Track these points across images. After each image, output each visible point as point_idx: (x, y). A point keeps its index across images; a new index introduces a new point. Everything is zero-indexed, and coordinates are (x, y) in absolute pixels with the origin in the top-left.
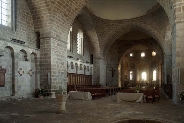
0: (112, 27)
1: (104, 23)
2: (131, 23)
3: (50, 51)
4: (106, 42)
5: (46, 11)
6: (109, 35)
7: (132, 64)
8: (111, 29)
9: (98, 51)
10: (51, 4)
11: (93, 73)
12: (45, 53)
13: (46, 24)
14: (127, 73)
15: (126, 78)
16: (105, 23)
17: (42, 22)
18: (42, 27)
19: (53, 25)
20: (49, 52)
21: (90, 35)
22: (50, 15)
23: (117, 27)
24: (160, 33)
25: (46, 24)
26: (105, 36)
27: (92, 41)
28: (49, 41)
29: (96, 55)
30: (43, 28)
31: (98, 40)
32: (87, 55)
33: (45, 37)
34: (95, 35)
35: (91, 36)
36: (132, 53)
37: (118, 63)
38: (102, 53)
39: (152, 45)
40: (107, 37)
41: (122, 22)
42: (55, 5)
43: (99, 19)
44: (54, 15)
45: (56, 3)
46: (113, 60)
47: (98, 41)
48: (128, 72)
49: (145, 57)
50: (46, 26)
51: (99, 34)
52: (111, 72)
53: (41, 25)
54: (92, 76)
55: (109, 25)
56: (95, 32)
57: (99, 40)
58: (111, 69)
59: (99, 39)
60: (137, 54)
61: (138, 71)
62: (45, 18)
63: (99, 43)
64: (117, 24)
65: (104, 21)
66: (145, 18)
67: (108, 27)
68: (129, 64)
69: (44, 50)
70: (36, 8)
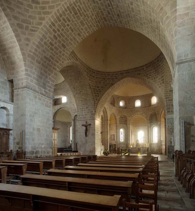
4: (37, 46)
6: (42, 29)
7: (122, 118)
8: (45, 13)
9: (22, 71)
14: (115, 130)
15: (114, 140)
23: (59, 4)
26: (34, 31)
29: (19, 80)
36: (122, 101)
39: (150, 78)
40: (37, 33)
46: (87, 108)
48: (116, 129)
49: (141, 107)
51: (16, 22)
52: (84, 127)
58: (85, 123)
59: (17, 36)
60: (130, 101)
61: (131, 127)
67: (38, 5)
68: (118, 118)
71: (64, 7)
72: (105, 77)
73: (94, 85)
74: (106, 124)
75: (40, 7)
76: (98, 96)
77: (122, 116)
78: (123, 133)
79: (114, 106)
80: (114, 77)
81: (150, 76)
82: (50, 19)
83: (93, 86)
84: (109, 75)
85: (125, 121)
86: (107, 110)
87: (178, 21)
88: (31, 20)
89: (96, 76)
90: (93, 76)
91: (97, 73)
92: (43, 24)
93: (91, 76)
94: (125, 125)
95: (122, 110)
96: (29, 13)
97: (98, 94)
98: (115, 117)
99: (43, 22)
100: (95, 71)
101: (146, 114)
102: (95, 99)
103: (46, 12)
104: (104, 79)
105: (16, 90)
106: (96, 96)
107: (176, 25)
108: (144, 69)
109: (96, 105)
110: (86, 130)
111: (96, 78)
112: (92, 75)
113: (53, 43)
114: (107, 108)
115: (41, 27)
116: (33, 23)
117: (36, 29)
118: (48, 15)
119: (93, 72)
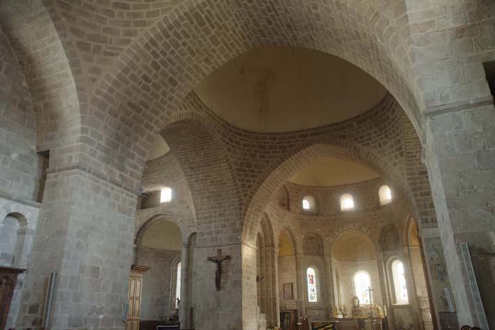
0: (144, 11)
4: (115, 83)
7: (310, 238)
14: (294, 272)
15: (293, 298)
26: (112, 54)
31: (69, 70)
37: (238, 223)
39: (368, 144)
46: (220, 215)
47: (71, 78)
48: (297, 268)
52: (213, 263)
54: (21, 271)
56: (51, 25)
58: (214, 254)
60: (326, 198)
61: (335, 264)
67: (126, 11)
68: (300, 238)
71: (179, 14)
72: (265, 143)
73: (239, 162)
74: (270, 254)
75: (128, 14)
76: (250, 187)
77: (310, 235)
78: (314, 279)
79: (289, 209)
80: (286, 143)
81: (370, 142)
82: (147, 33)
83: (236, 163)
84: (275, 139)
85: (319, 247)
86: (271, 219)
87: (415, 35)
88: (108, 36)
89: (243, 142)
90: (236, 142)
91: (245, 136)
92: (131, 43)
93: (232, 141)
94: (318, 258)
95: (310, 220)
96: (105, 24)
97: (249, 181)
98: (292, 235)
99: (133, 39)
100: (243, 130)
101: (370, 229)
102: (242, 194)
103: (141, 21)
104: (263, 147)
106: (243, 186)
107: (410, 42)
108: (352, 126)
109: (243, 207)
110: (219, 272)
111: (244, 145)
112: (234, 140)
113: (150, 76)
114: (271, 215)
115: (129, 46)
117: (118, 51)
118: (145, 28)
119: (236, 133)
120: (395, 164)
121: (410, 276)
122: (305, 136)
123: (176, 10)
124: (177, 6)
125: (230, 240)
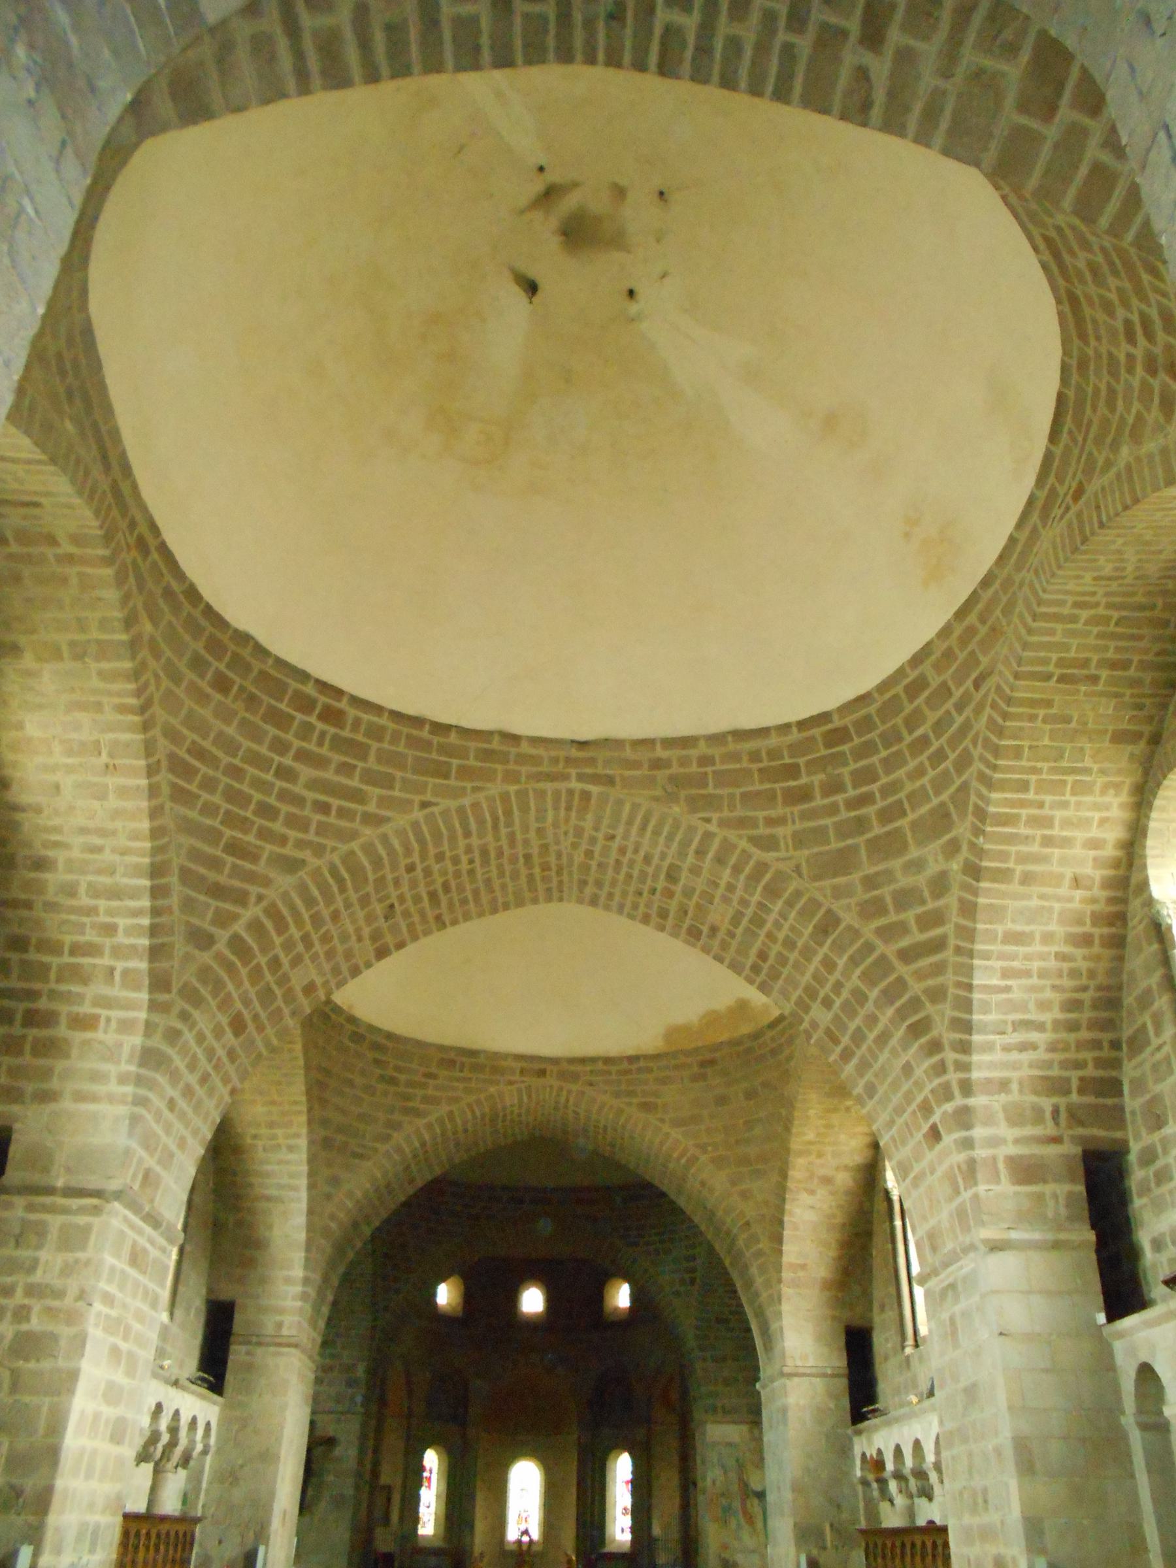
0: (420, 1093)
1: (370, 1055)
2: (561, 1089)
3: (73, 1318)
5: (137, 988)
8: (407, 1111)
10: (180, 946)
11: (204, 1485)
12: (18, 1335)
13: (97, 1077)
16: (377, 1062)
17: (67, 1056)
18: (46, 1097)
19: (151, 1095)
20: (65, 1332)
21: (255, 1137)
22: (156, 1018)
23: (456, 1100)
24: (745, 1195)
25: (97, 1077)
26: (361, 1157)
27: (253, 1180)
28: (87, 1230)
30: (53, 1106)
31: (303, 1182)
32: (188, 1310)
33: (60, 1183)
34: (292, 1142)
35: (260, 1143)
38: (312, 1292)
41: (495, 1070)
42: (206, 957)
43: (350, 1027)
44: (179, 1025)
45: (221, 946)
47: (304, 1195)
50: (94, 1098)
53: (47, 1074)
54: (197, 1520)
55: (402, 1077)
57: (311, 1187)
59: (311, 1174)
62: (105, 1036)
63: (311, 1212)
64: (458, 1080)
65: (376, 1047)
66: (649, 1070)
67: (392, 1089)
69: (19, 1298)
70: (55, 948)
71: (473, 1112)
99: (395, 1135)
105: (243, 1348)
116: (364, 1136)
120: (677, 1294)
121: (641, 1486)
122: (521, 1202)
123: (470, 1106)
124: (472, 1098)
125: (338, 1402)
